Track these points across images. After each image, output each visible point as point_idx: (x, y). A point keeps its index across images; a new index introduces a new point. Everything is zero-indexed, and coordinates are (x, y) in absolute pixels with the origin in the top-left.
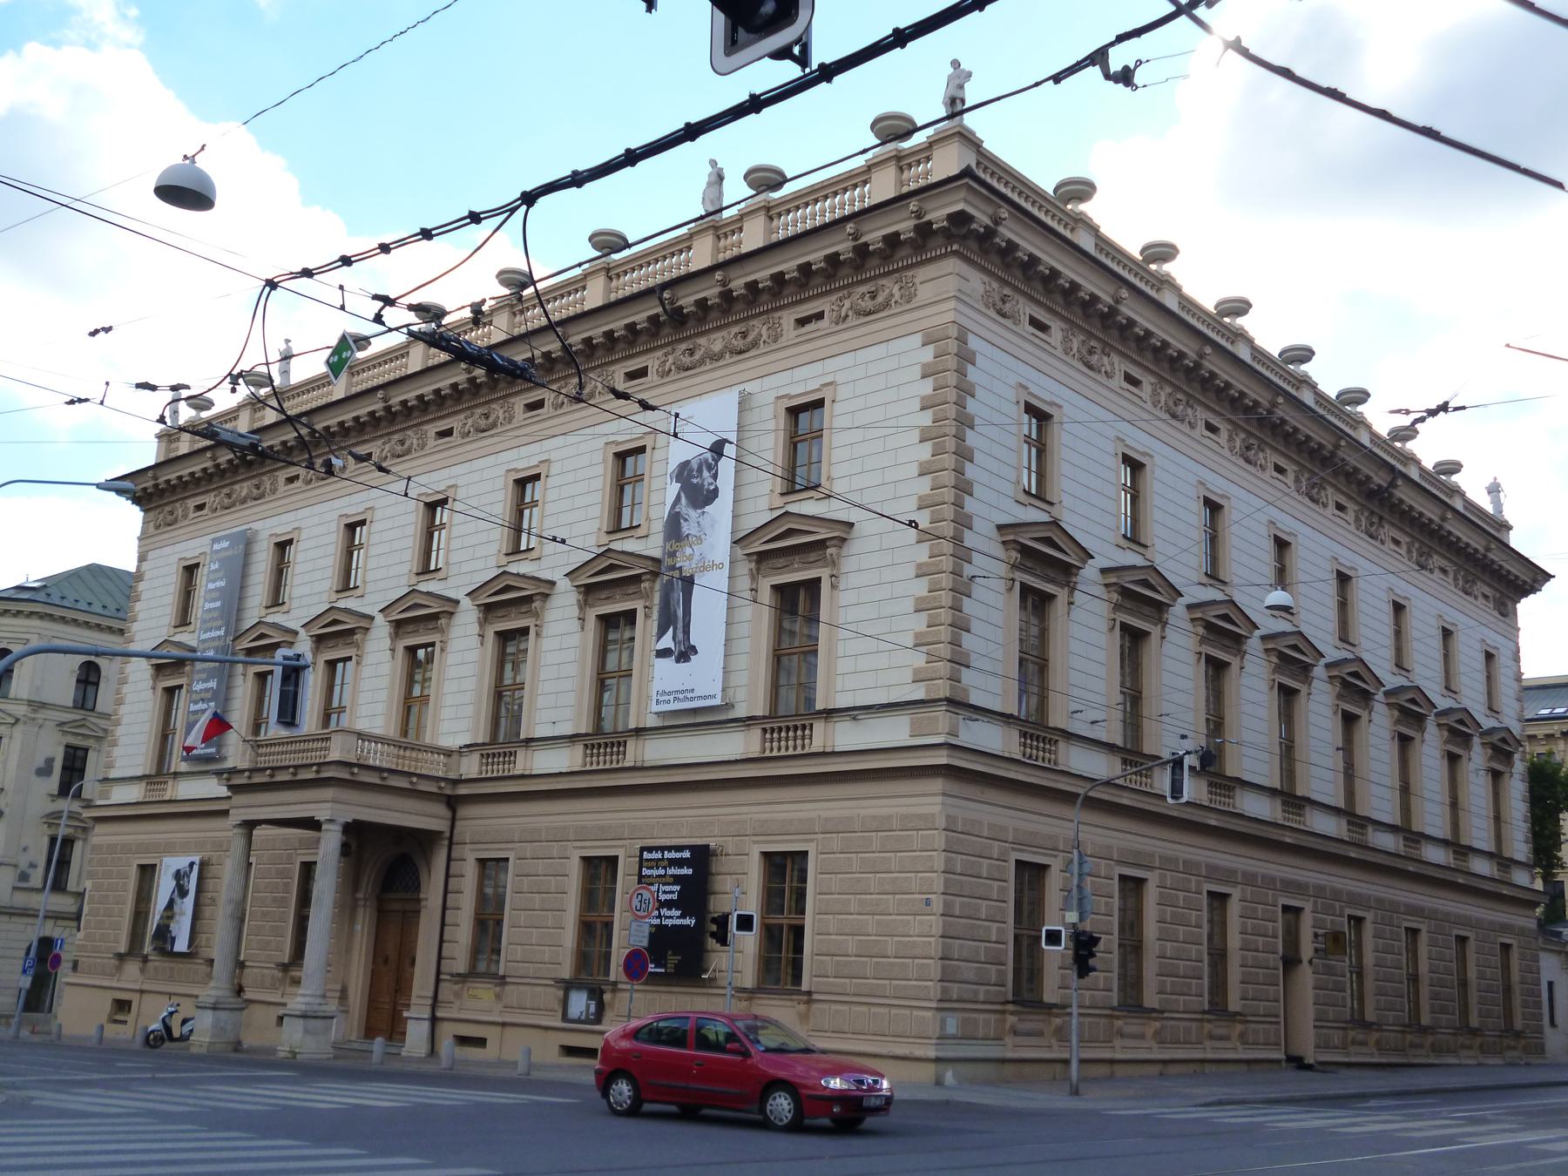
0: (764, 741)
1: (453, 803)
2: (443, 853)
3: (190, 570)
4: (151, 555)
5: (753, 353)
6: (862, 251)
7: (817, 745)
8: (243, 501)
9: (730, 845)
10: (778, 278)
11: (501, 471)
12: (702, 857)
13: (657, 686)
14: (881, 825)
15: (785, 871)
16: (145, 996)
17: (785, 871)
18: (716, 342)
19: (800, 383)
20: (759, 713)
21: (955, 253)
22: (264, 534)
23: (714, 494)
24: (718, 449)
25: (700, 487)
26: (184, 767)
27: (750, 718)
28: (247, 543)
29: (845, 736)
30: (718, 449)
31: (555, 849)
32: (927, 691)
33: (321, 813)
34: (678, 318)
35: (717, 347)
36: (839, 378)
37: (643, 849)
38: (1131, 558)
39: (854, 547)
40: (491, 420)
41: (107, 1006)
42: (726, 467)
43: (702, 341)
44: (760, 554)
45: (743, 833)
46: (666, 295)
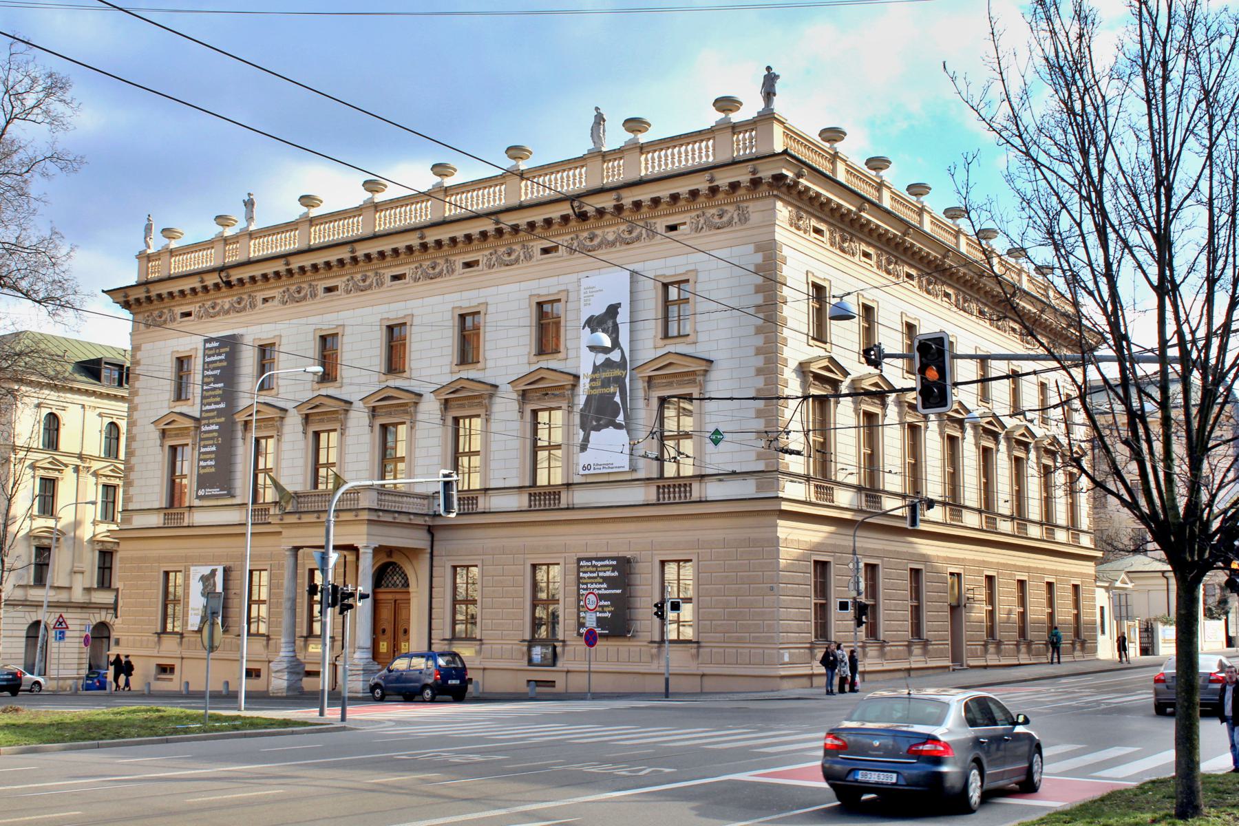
0: (658, 493)
1: (431, 530)
3: (182, 362)
4: (144, 347)
5: (636, 245)
7: (695, 496)
8: (227, 312)
11: (450, 307)
12: (624, 566)
16: (705, 679)
20: (655, 476)
21: (776, 196)
22: (248, 339)
26: (197, 503)
27: (648, 479)
28: (231, 344)
32: (767, 465)
33: (360, 542)
34: (583, 216)
35: (611, 237)
37: (579, 560)
40: (437, 270)
41: (153, 670)
43: (598, 232)
46: (576, 204)
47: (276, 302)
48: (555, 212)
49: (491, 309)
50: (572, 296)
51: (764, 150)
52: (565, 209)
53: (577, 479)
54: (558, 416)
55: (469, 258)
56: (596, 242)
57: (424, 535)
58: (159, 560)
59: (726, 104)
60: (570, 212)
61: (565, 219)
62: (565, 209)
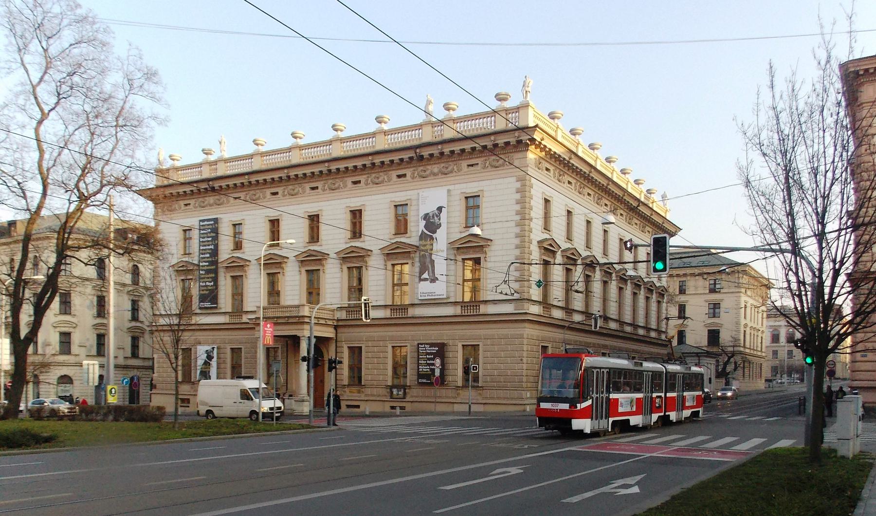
2: (334, 345)
6: (496, 146)
9: (451, 342)
10: (463, 151)
13: (420, 290)
14: (506, 337)
15: (472, 350)
17: (472, 350)
18: (436, 168)
19: (471, 188)
23: (439, 226)
24: (440, 209)
25: (433, 223)
29: (491, 309)
30: (440, 209)
31: (381, 343)
34: (421, 158)
36: (485, 189)
38: (568, 245)
39: (493, 248)
42: (444, 215)
43: (429, 167)
44: (458, 248)
45: (456, 340)
46: (418, 151)
47: (479, 168)
48: (405, 156)
49: (486, 194)
50: (414, 203)
51: (522, 124)
52: (411, 154)
53: (417, 302)
54: (406, 268)
55: (400, 172)
56: (428, 172)
57: (332, 330)
58: (392, 339)
59: (500, 98)
60: (414, 155)
61: (411, 158)
62: (411, 154)
